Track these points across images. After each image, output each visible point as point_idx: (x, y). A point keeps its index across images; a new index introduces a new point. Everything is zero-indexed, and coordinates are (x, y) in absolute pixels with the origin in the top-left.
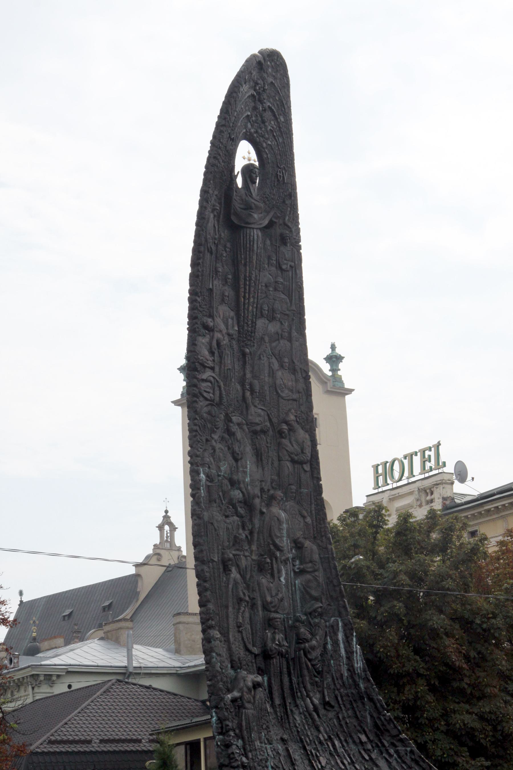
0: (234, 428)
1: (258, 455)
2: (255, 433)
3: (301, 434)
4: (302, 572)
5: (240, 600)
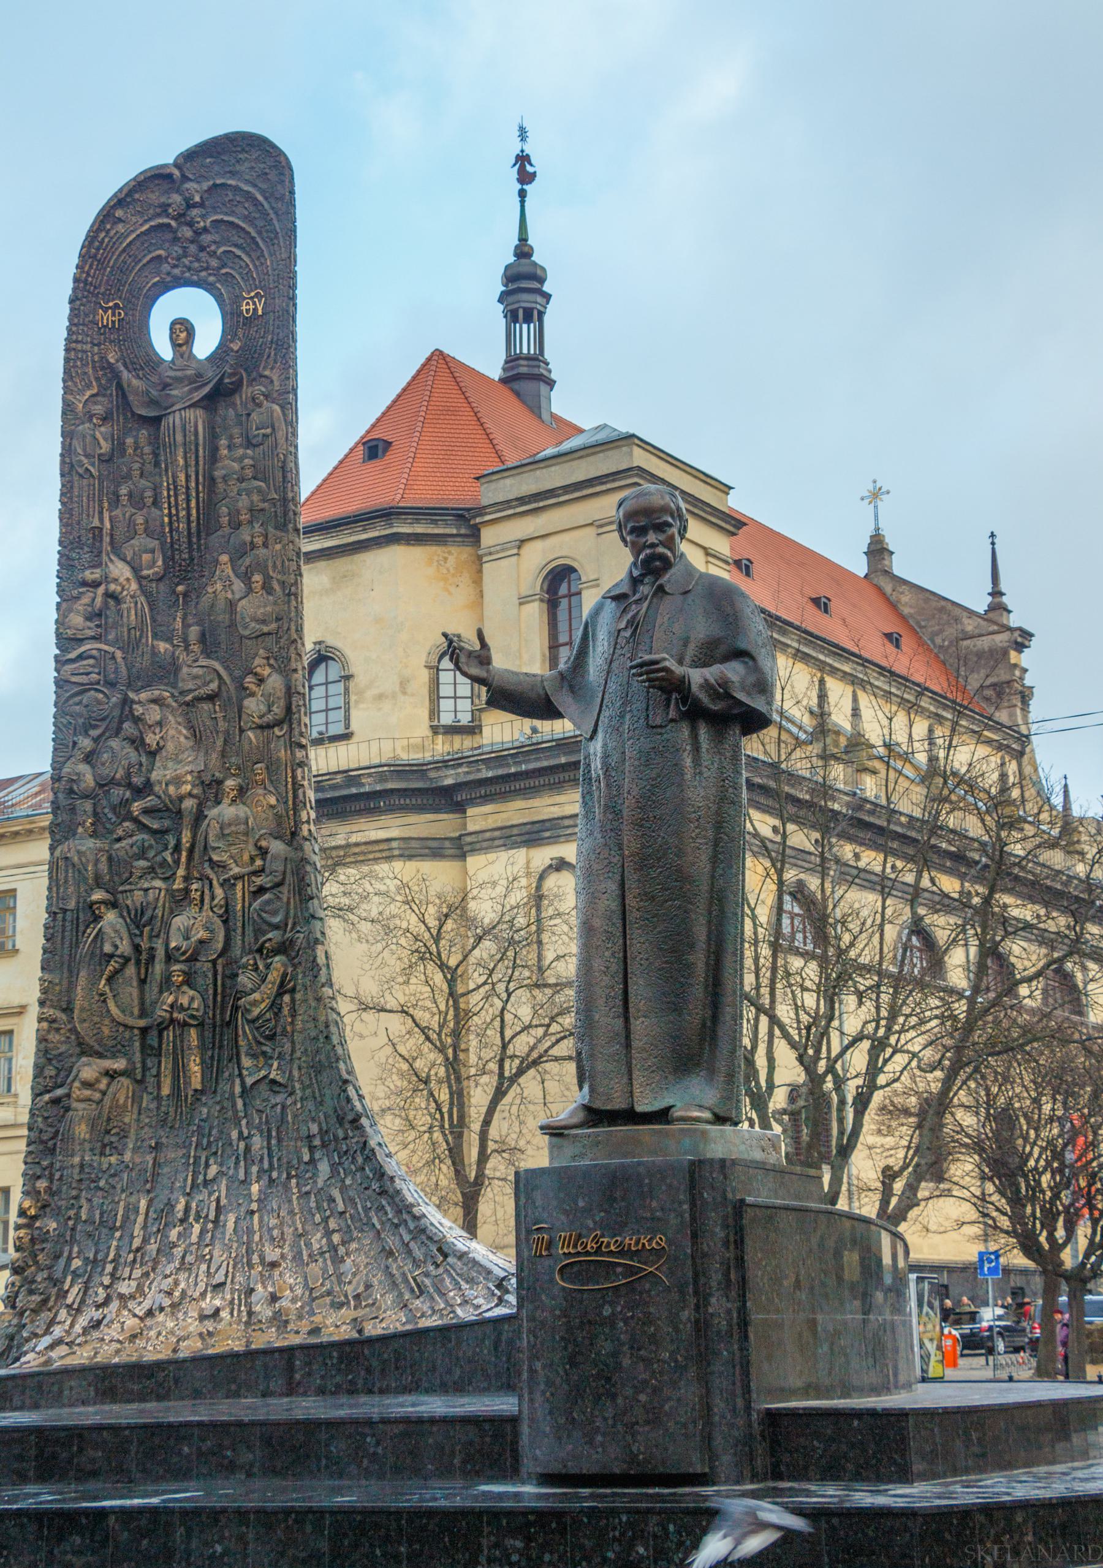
0: (138, 710)
1: (197, 736)
2: (187, 704)
3: (275, 682)
4: (261, 890)
5: (111, 956)
